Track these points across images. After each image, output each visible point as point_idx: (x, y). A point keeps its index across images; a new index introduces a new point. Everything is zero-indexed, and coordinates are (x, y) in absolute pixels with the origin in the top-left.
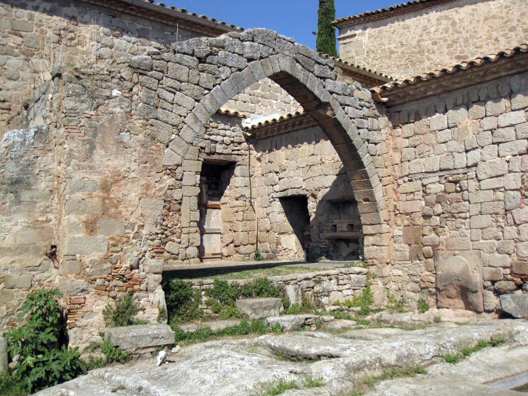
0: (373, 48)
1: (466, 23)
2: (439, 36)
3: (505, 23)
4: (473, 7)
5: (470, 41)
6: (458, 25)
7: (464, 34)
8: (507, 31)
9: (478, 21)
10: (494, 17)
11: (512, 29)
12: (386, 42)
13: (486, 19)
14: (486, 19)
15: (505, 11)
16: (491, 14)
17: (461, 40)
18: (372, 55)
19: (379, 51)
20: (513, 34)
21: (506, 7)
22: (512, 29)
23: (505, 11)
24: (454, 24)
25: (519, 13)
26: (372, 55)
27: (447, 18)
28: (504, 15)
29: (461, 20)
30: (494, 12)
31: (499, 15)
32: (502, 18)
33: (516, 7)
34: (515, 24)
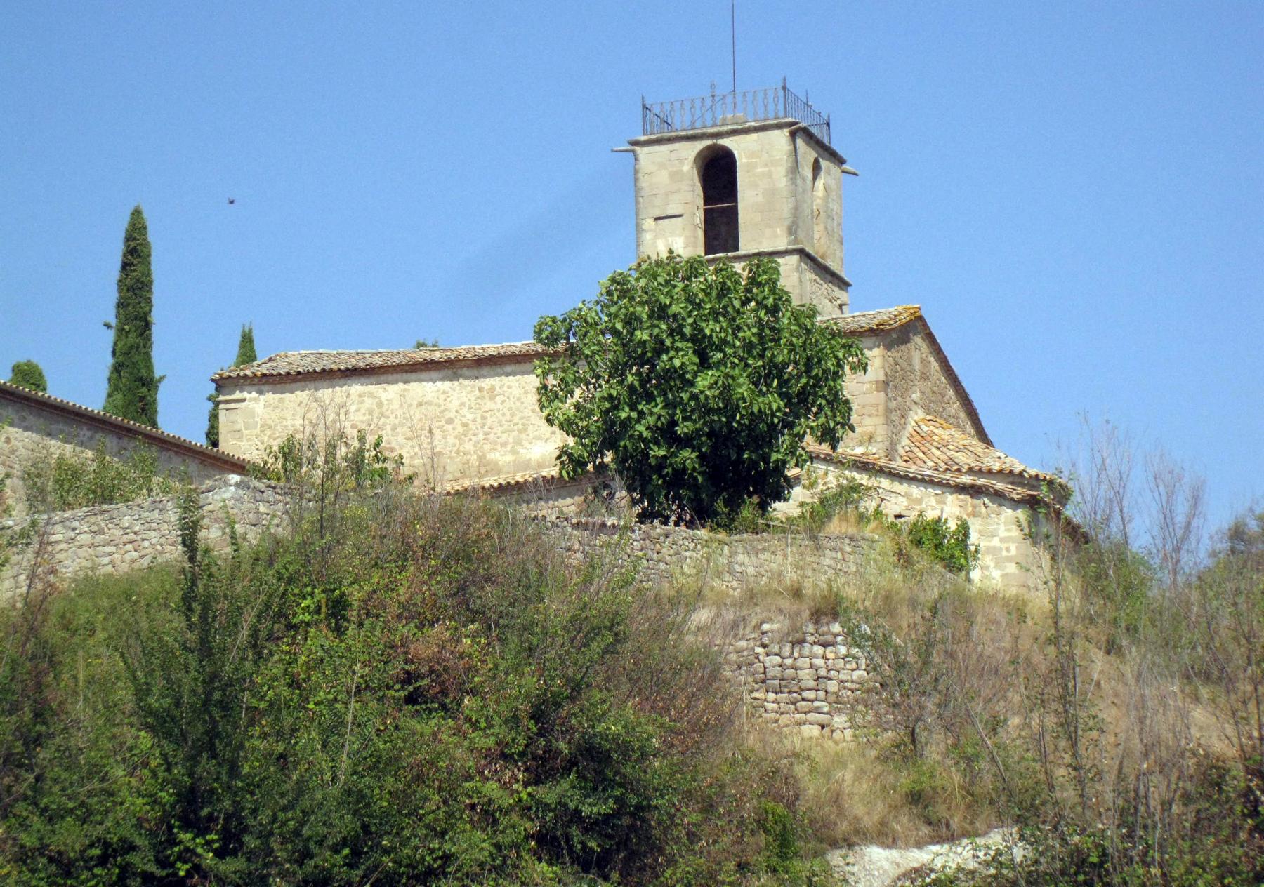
0: (269, 422)
1: (395, 405)
2: (361, 418)
3: (442, 412)
4: (405, 386)
5: (399, 430)
6: (385, 407)
7: (392, 420)
8: (443, 423)
9: (411, 405)
10: (429, 403)
11: (450, 421)
12: (289, 417)
13: (420, 404)
14: (420, 404)
15: (442, 397)
16: (426, 399)
17: (389, 427)
18: (268, 432)
19: (279, 427)
20: (450, 427)
21: (444, 393)
22: (450, 421)
23: (442, 397)
24: (380, 404)
25: (458, 403)
26: (268, 432)
27: (371, 395)
28: (441, 402)
29: (390, 401)
30: (429, 397)
31: (436, 401)
32: (439, 406)
33: (455, 394)
34: (452, 415)
